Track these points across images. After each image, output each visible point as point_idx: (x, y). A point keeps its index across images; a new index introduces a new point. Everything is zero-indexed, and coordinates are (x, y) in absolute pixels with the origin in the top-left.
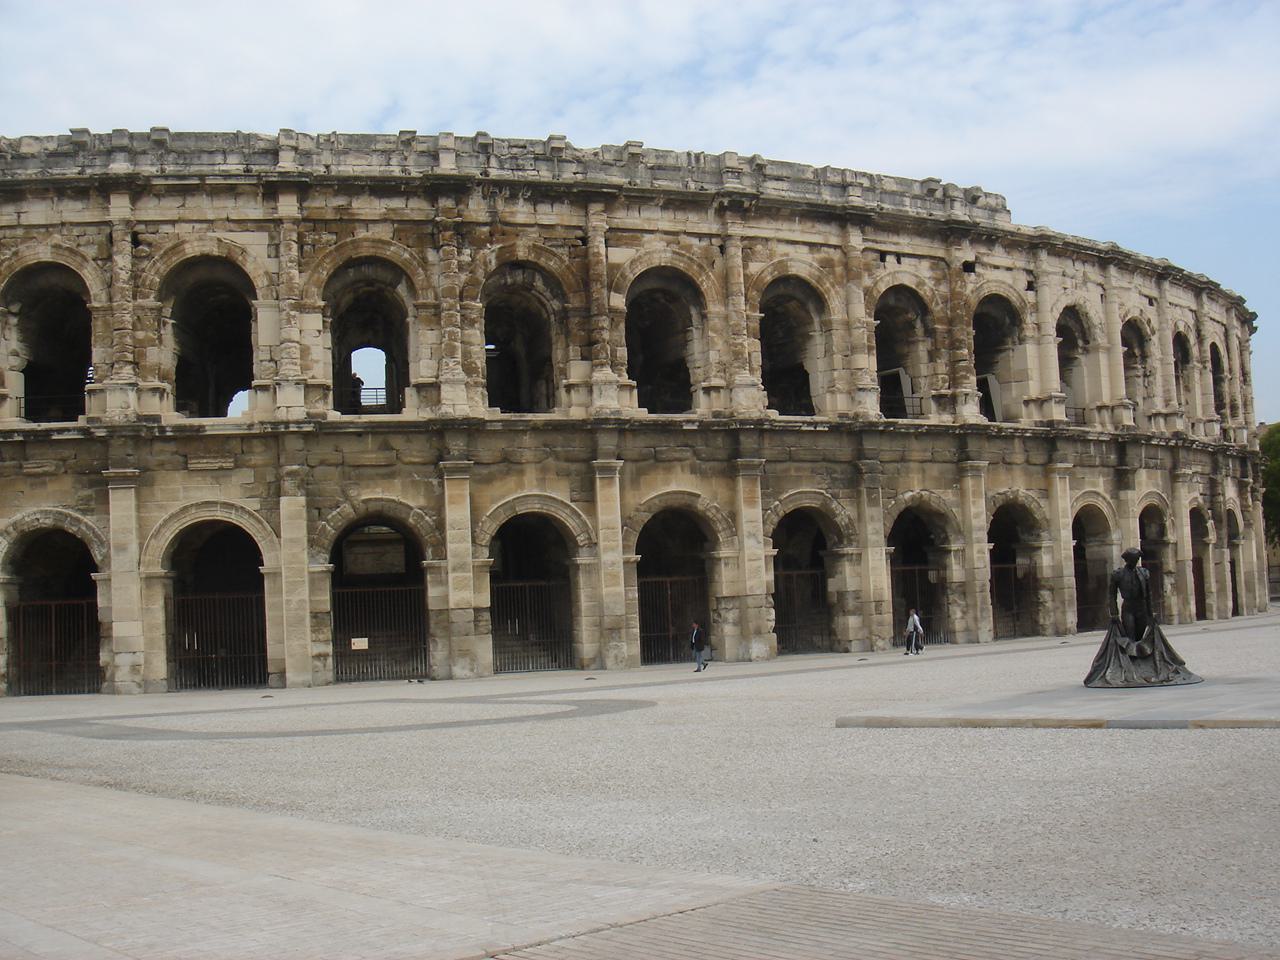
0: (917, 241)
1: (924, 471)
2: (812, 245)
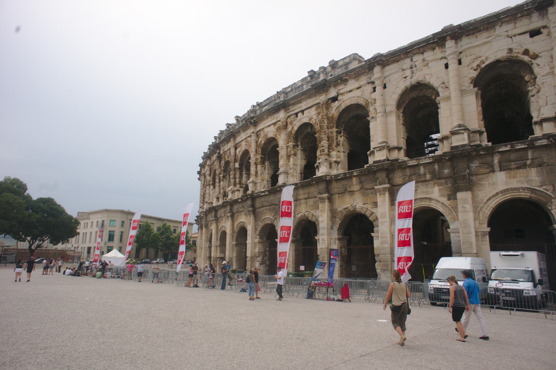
0: (309, 100)
1: (306, 203)
2: (274, 124)
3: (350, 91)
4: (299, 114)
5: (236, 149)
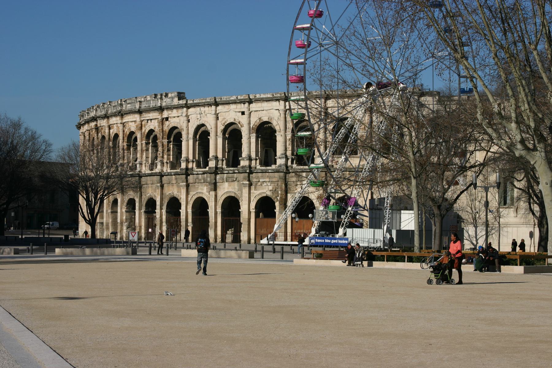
3: (174, 117)
4: (149, 121)
5: (110, 129)
